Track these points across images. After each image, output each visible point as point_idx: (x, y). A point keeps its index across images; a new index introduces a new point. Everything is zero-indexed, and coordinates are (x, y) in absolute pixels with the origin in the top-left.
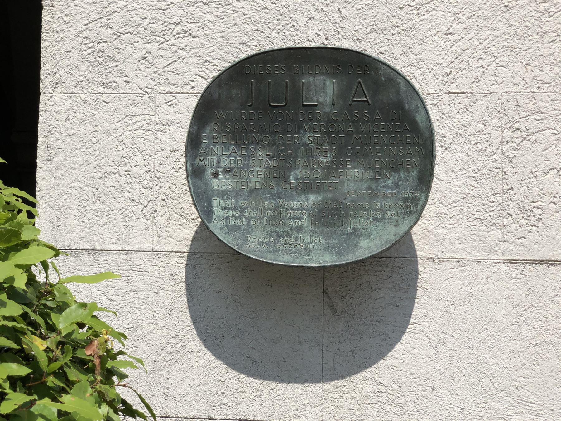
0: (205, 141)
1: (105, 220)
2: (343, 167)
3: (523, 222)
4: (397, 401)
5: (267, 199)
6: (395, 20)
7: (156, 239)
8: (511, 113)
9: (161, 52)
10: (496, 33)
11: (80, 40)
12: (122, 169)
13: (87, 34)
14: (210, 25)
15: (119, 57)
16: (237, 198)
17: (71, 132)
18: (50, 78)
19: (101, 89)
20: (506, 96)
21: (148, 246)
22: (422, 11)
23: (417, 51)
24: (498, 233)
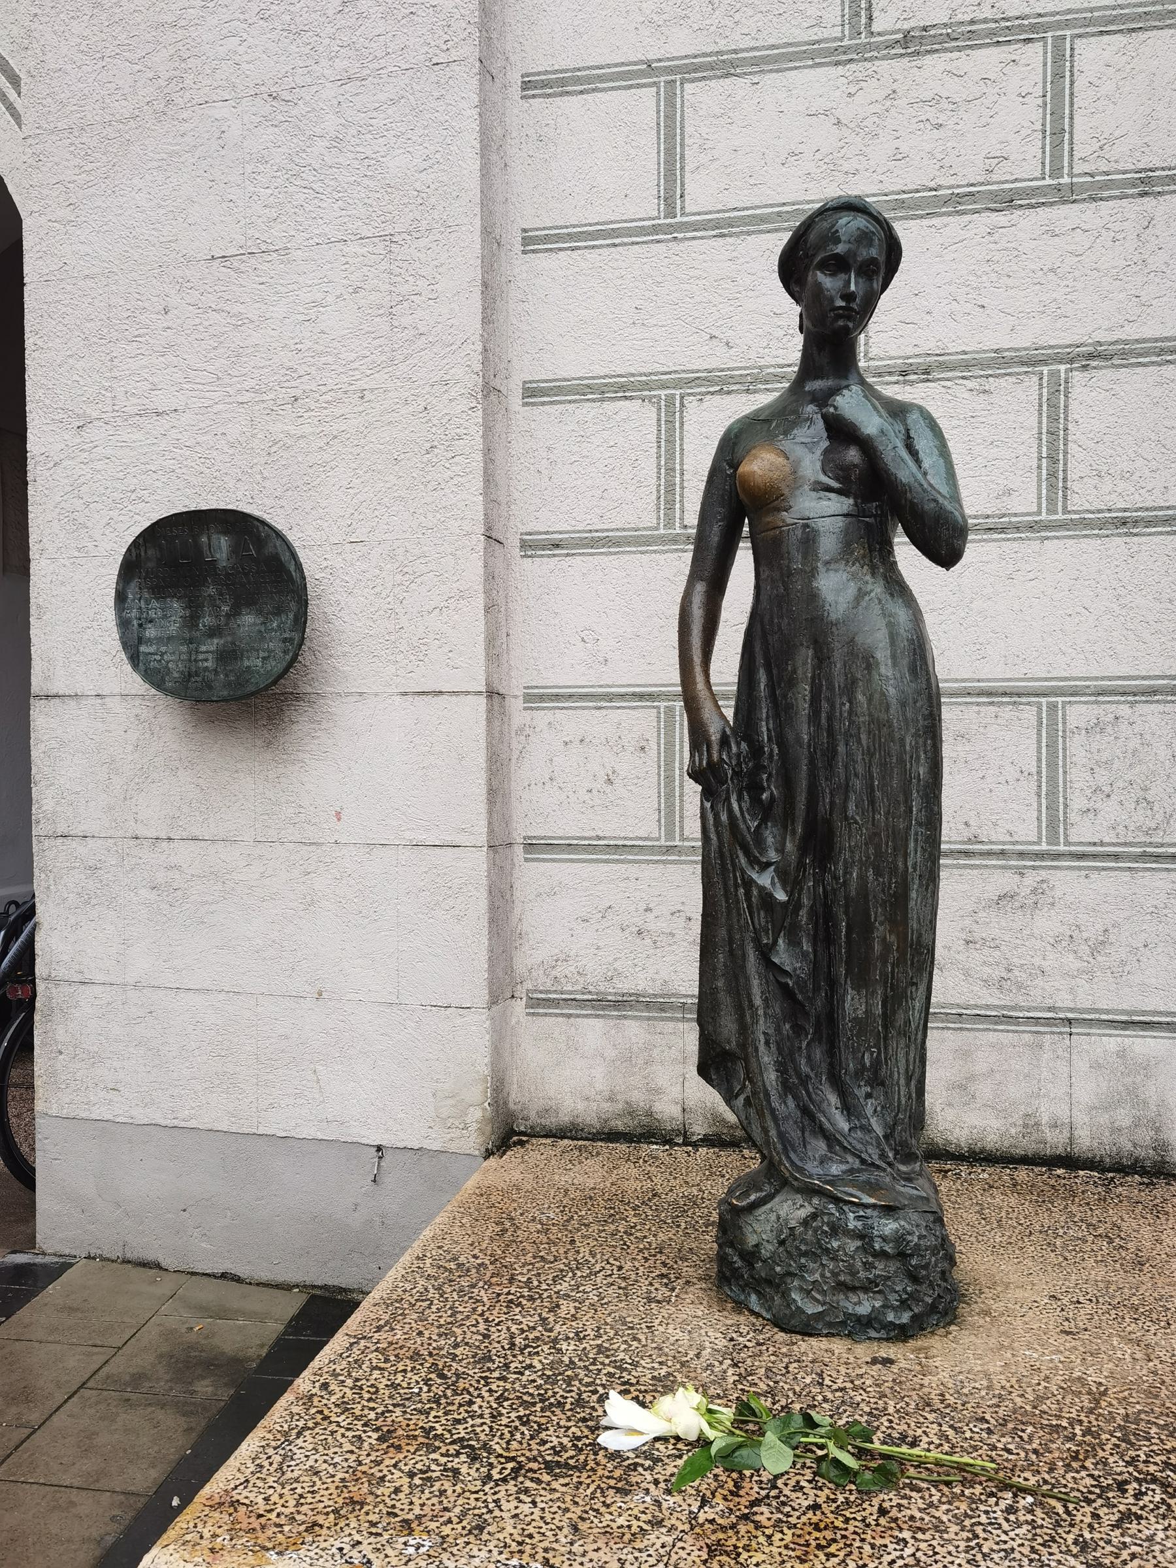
0: (130, 596)
1: (84, 669)
2: (240, 614)
3: (412, 658)
4: (313, 821)
5: (182, 644)
6: (306, 478)
7: (123, 685)
8: (401, 558)
9: (121, 518)
10: (388, 485)
11: (57, 510)
12: (95, 623)
13: (63, 504)
14: (159, 491)
15: (89, 524)
16: (157, 644)
17: (55, 593)
18: (37, 546)
19: (76, 554)
20: (397, 543)
21: (117, 691)
22: (328, 468)
23: (323, 505)
24: (392, 669)
